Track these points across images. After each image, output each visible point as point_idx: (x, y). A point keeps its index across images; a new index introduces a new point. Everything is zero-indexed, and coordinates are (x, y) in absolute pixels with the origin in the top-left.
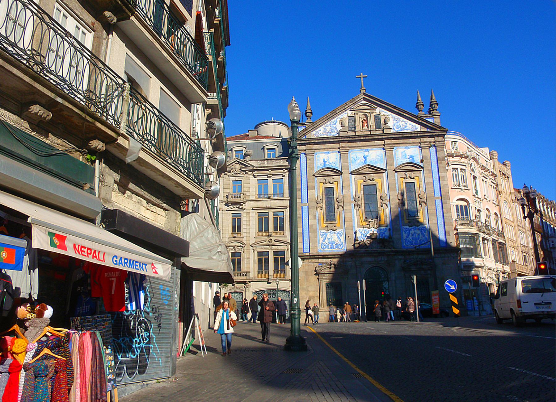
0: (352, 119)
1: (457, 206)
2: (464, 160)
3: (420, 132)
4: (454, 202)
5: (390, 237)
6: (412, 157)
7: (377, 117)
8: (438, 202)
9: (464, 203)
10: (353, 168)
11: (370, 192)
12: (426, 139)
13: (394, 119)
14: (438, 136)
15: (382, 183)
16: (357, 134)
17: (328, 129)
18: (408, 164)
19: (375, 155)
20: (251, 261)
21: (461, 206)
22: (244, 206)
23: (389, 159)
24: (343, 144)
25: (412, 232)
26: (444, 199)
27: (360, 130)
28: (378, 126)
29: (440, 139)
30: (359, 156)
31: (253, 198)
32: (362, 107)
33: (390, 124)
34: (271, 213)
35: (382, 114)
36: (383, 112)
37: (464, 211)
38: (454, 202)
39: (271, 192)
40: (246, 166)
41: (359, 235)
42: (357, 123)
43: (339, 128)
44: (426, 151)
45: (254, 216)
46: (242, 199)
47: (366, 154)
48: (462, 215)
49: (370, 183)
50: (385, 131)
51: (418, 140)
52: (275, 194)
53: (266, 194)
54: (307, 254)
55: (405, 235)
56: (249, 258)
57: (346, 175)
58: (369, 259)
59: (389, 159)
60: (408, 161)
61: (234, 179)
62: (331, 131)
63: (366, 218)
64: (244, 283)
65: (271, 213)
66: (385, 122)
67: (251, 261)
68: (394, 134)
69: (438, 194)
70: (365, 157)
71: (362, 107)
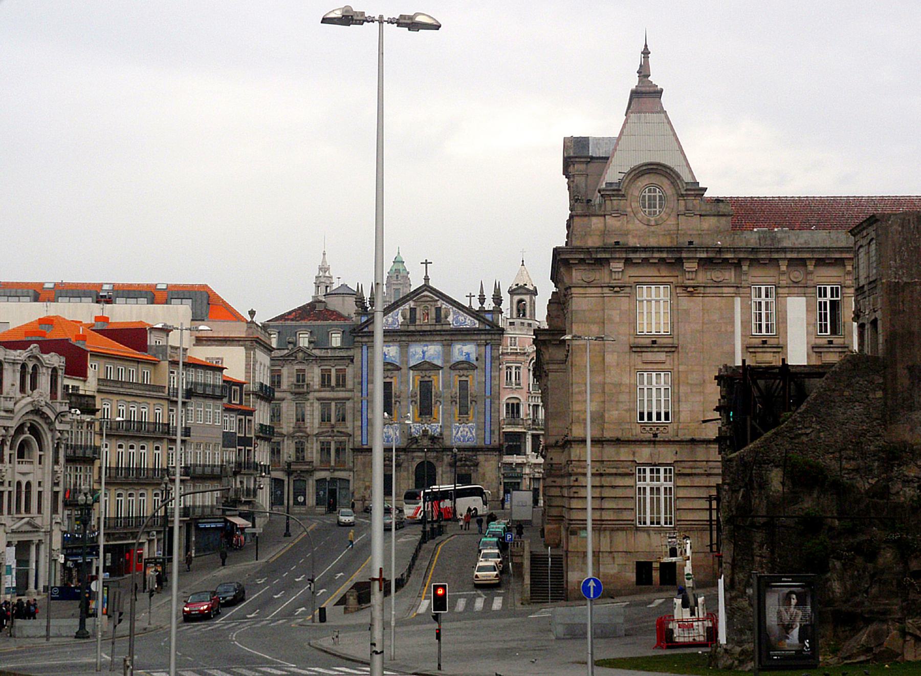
0: (413, 310)
1: (507, 405)
2: (520, 358)
3: (478, 330)
4: (504, 401)
5: (441, 434)
6: (468, 354)
7: (438, 310)
8: (488, 400)
9: (515, 402)
10: (412, 364)
11: (426, 389)
12: (483, 337)
13: (454, 313)
14: (494, 334)
15: (439, 381)
16: (418, 328)
17: (390, 320)
18: (462, 362)
19: (433, 351)
20: (315, 451)
21: (513, 404)
22: (308, 397)
23: (447, 354)
24: (404, 338)
25: (461, 429)
26: (495, 397)
27: (424, 322)
28: (438, 319)
29: (497, 337)
30: (419, 352)
31: (317, 387)
32: (423, 299)
33: (450, 319)
34: (333, 404)
35: (444, 306)
36: (445, 306)
37: (514, 409)
38: (504, 401)
39: (333, 383)
40: (309, 355)
41: (413, 430)
42: (418, 316)
43: (401, 320)
44: (483, 348)
45: (317, 405)
46: (305, 390)
47: (425, 348)
48: (513, 412)
49: (427, 379)
50: (446, 327)
51: (476, 338)
52: (338, 385)
53: (329, 385)
54: (365, 447)
55: (454, 432)
56: (312, 448)
57: (404, 371)
58: (420, 454)
59: (447, 354)
60: (462, 358)
61: (297, 367)
62: (393, 323)
63: (421, 414)
64: (307, 471)
65: (333, 404)
66: (446, 317)
67: (315, 451)
68: (452, 330)
69: (488, 394)
70: (424, 352)
71: (423, 299)
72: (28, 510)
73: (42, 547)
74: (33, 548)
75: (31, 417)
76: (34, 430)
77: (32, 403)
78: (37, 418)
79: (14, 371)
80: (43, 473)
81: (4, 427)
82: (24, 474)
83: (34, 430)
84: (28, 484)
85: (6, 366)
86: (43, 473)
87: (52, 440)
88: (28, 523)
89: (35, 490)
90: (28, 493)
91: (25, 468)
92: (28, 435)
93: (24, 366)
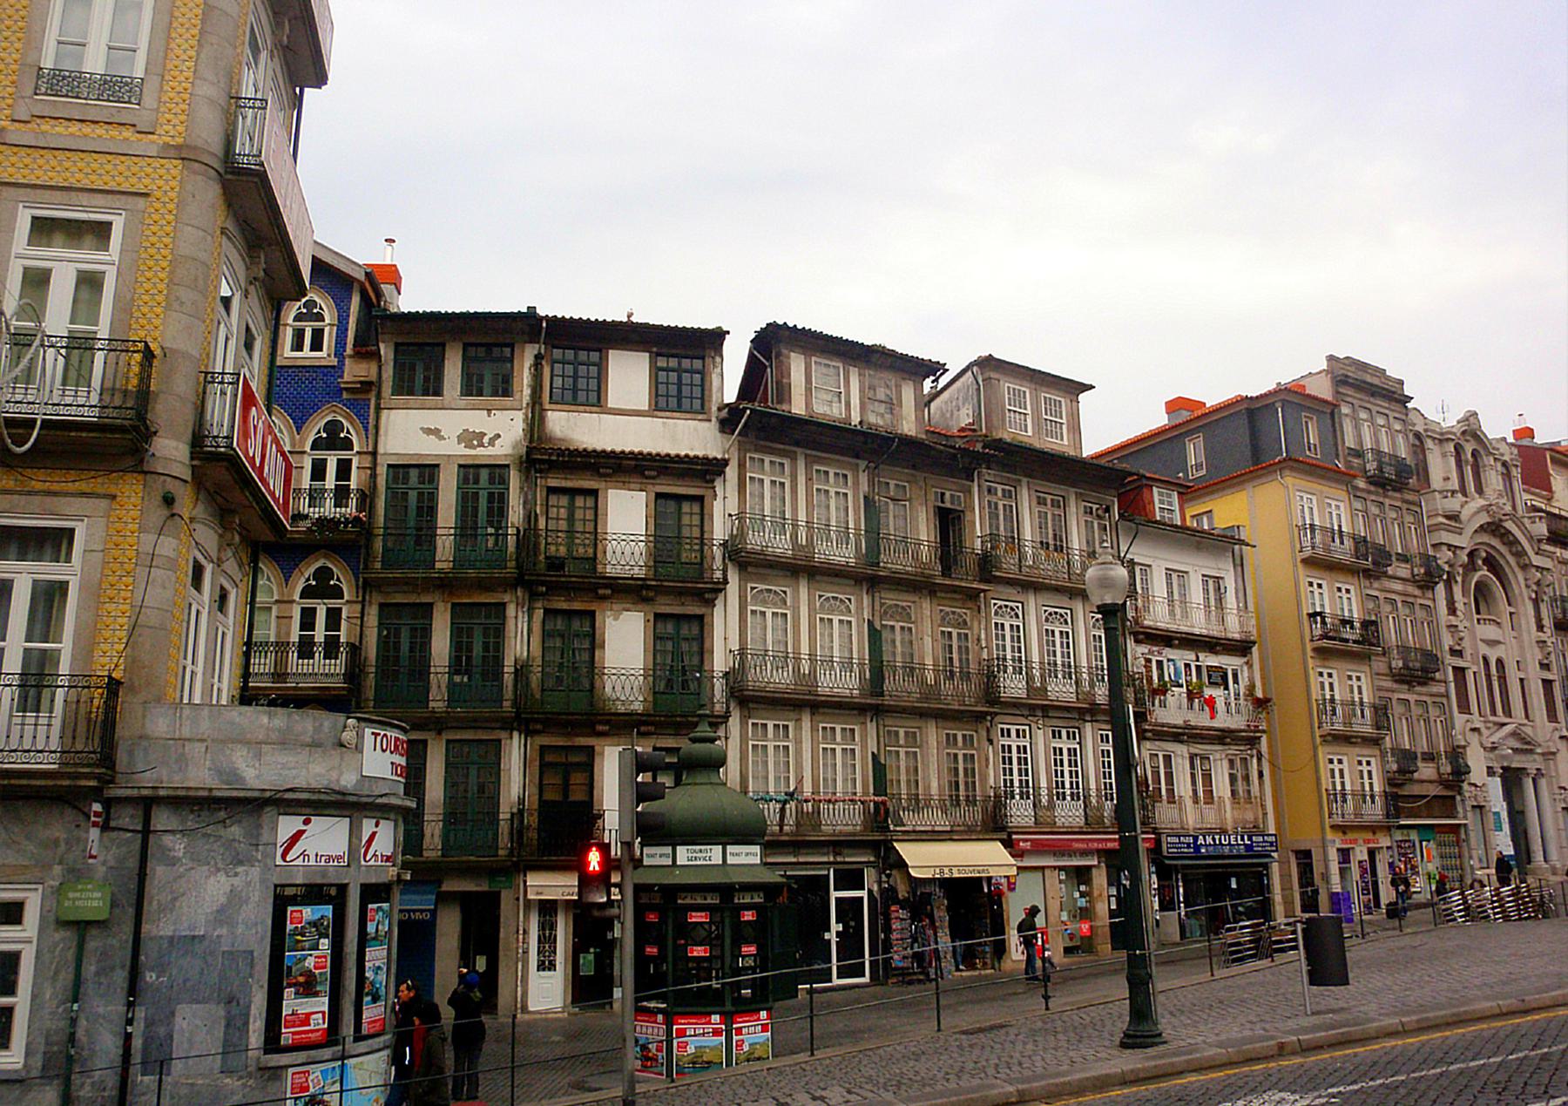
72: (1508, 712)
73: (1543, 782)
74: (1529, 784)
75: (1486, 538)
76: (1491, 563)
77: (1486, 509)
78: (1495, 542)
79: (1444, 455)
80: (1522, 648)
81: (1449, 546)
82: (1492, 643)
83: (1491, 563)
84: (1500, 663)
85: (1429, 444)
86: (1522, 648)
87: (1528, 586)
88: (1514, 734)
89: (1513, 676)
90: (1503, 679)
91: (1490, 631)
92: (1485, 572)
93: (1458, 449)
